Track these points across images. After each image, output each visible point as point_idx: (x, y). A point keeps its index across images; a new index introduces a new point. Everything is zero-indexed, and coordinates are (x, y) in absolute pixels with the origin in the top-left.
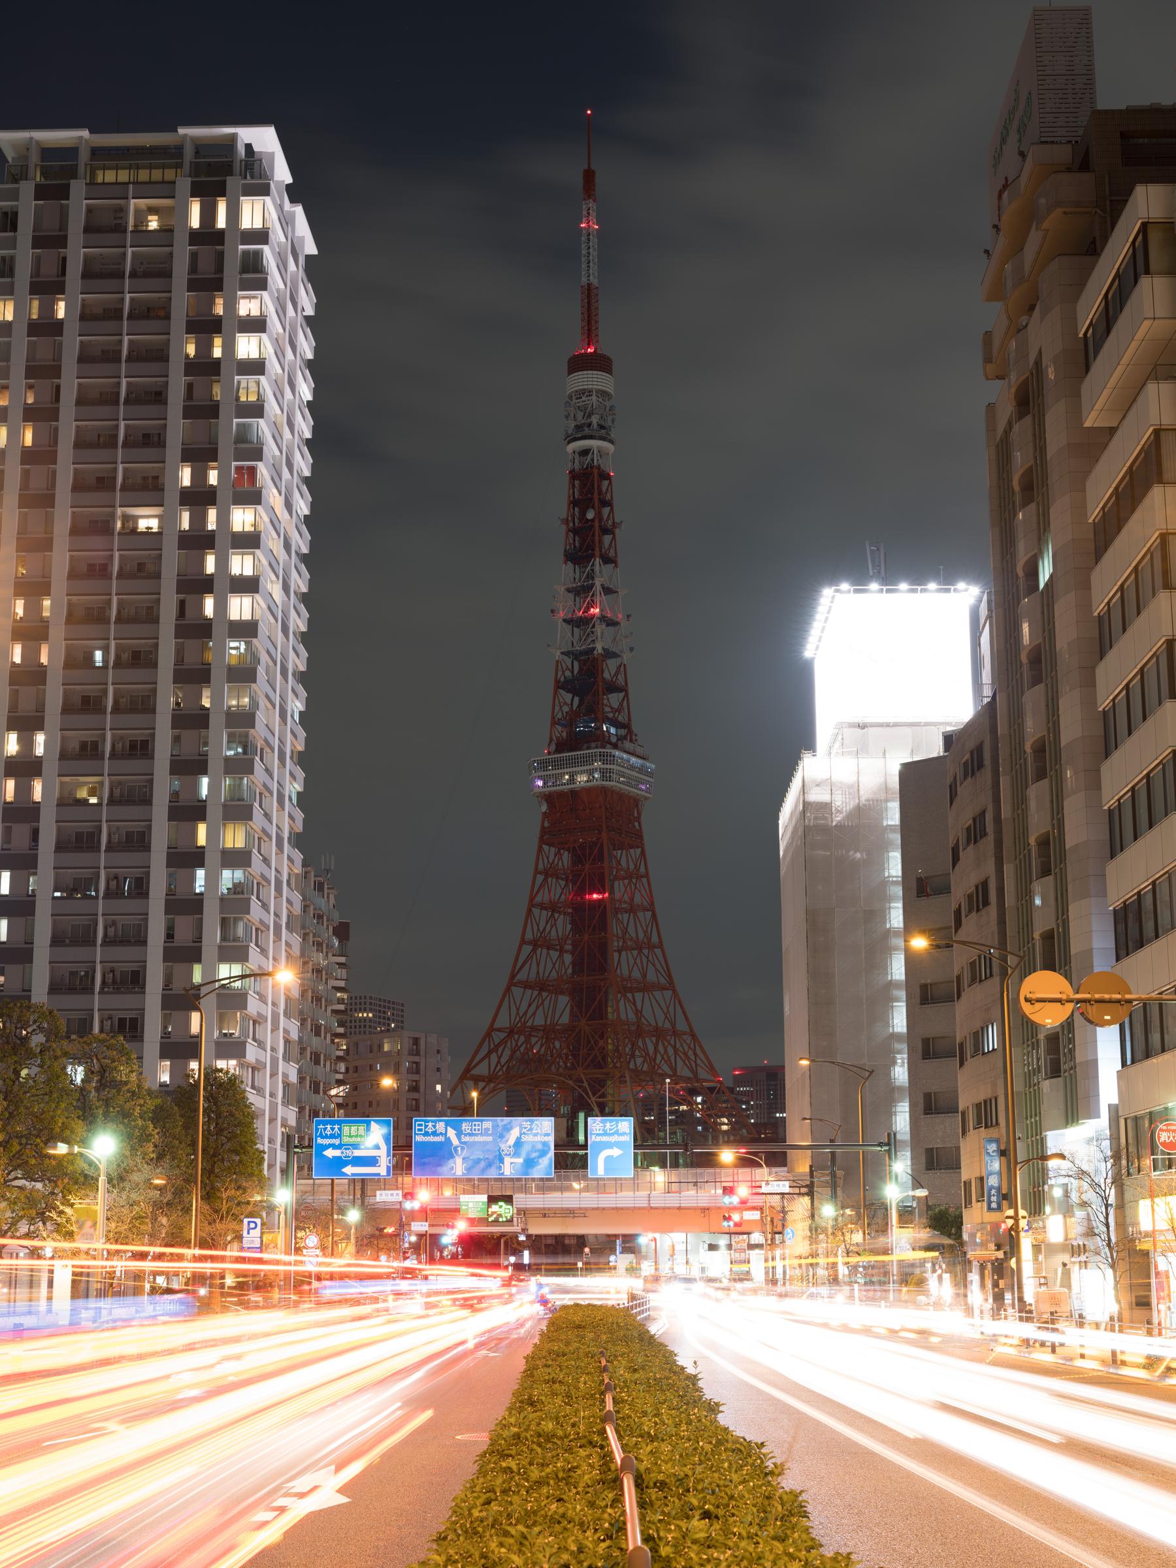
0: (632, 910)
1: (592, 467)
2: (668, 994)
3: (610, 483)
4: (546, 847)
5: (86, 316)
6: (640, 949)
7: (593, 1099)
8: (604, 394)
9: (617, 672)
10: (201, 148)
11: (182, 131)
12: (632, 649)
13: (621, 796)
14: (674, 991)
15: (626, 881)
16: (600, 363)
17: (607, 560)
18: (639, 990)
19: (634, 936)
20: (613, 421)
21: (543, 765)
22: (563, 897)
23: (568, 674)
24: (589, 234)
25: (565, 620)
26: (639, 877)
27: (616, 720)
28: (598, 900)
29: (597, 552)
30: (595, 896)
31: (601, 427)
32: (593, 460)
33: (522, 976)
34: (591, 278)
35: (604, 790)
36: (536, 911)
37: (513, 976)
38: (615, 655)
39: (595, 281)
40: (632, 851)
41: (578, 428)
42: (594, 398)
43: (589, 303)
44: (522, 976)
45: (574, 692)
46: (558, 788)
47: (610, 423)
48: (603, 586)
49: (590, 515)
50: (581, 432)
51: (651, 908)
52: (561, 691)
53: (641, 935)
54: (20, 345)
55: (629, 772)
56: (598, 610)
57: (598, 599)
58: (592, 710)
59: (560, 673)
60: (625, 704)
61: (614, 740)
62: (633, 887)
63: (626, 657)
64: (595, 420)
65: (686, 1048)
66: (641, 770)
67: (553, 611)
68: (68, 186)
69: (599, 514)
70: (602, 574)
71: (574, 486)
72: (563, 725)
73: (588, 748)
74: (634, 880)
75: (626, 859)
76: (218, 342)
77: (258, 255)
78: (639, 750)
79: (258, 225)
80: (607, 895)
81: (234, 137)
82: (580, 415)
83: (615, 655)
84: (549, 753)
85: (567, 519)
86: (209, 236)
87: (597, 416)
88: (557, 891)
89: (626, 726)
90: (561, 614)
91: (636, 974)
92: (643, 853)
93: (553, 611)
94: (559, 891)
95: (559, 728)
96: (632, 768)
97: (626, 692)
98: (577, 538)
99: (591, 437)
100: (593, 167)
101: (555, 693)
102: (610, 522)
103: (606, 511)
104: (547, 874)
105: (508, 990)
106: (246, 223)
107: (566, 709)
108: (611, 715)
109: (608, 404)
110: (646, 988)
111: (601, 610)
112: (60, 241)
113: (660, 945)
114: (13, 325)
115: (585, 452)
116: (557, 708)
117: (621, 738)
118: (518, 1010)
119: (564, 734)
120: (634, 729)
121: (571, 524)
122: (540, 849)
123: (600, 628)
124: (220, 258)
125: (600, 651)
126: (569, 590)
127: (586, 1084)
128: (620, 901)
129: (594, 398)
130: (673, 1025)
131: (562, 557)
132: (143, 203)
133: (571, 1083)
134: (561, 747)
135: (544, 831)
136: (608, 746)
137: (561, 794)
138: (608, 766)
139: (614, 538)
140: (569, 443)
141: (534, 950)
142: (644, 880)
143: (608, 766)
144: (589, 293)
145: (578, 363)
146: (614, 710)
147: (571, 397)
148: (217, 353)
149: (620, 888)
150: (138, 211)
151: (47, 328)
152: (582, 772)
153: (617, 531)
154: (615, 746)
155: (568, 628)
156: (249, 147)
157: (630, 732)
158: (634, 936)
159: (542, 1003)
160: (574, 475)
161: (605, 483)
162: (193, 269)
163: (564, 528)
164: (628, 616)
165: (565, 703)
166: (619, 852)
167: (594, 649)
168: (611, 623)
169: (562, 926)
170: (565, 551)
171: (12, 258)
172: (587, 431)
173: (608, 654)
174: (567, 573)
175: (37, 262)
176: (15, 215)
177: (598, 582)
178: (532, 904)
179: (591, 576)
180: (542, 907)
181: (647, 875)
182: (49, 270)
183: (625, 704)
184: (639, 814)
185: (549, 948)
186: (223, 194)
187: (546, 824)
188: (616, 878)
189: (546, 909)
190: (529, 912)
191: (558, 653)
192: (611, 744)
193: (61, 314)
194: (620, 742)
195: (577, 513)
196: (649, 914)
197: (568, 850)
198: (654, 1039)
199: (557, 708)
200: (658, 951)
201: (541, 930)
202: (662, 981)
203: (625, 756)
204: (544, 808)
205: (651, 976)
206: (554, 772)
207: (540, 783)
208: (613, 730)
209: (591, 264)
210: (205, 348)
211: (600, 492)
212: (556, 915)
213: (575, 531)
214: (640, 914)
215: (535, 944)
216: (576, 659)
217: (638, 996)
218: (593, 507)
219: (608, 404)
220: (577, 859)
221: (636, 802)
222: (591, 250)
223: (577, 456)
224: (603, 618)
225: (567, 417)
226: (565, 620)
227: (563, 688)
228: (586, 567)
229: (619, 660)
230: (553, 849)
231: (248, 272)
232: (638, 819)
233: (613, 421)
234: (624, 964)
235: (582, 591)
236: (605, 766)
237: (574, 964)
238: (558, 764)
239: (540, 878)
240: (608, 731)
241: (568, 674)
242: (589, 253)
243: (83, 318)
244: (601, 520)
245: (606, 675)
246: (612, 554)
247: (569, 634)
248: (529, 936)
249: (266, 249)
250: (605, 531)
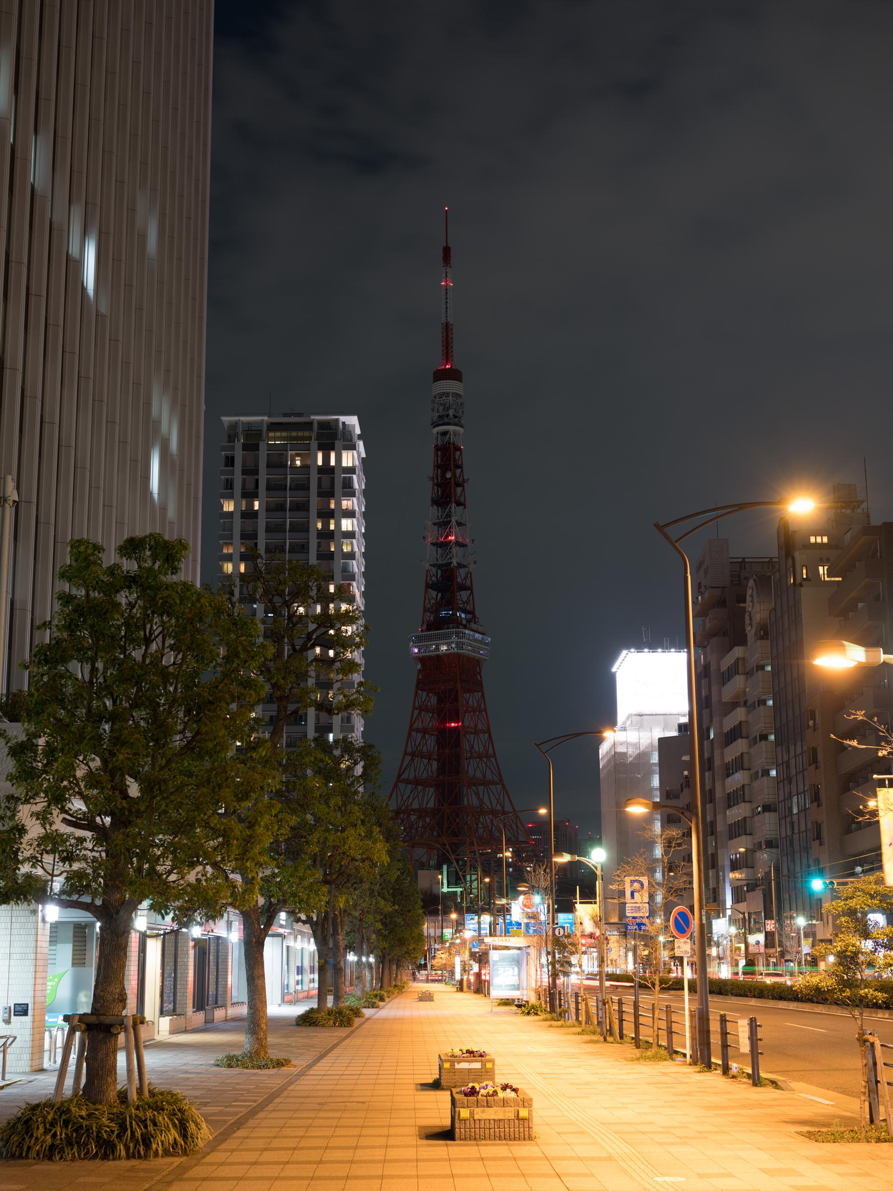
0: (476, 733)
1: (449, 443)
2: (499, 787)
3: (461, 454)
4: (420, 692)
5: (269, 508)
6: (481, 758)
7: (453, 857)
8: (457, 395)
9: (466, 578)
10: (324, 425)
11: (312, 417)
12: (475, 562)
13: (469, 659)
14: (503, 785)
15: (472, 714)
16: (454, 375)
17: (459, 504)
18: (481, 785)
19: (477, 750)
20: (463, 413)
21: (419, 639)
22: (431, 723)
23: (434, 579)
24: (447, 290)
25: (432, 544)
26: (480, 711)
27: (466, 609)
28: (455, 727)
29: (453, 500)
30: (453, 725)
31: (455, 417)
32: (450, 438)
33: (405, 776)
34: (448, 318)
35: (458, 655)
36: (414, 734)
37: (399, 776)
38: (464, 566)
39: (451, 320)
40: (476, 694)
41: (439, 417)
42: (451, 398)
43: (447, 335)
44: (405, 776)
45: (438, 590)
46: (427, 654)
47: (461, 414)
48: (457, 522)
49: (448, 475)
50: (442, 420)
51: (488, 731)
52: (430, 590)
53: (481, 749)
54: (237, 522)
55: (474, 643)
56: (453, 538)
57: (453, 530)
58: (449, 602)
59: (429, 578)
60: (471, 598)
61: (464, 622)
62: (476, 717)
63: (472, 567)
64: (451, 412)
65: (511, 822)
66: (481, 642)
67: (424, 538)
68: (258, 444)
69: (454, 475)
70: (457, 513)
71: (437, 455)
72: (432, 613)
73: (448, 628)
74: (477, 713)
75: (472, 699)
76: (332, 522)
77: (351, 479)
78: (480, 629)
79: (350, 465)
80: (460, 724)
81: (337, 420)
82: (441, 408)
83: (464, 566)
84: (422, 631)
85: (433, 478)
86: (326, 469)
88: (428, 720)
89: (472, 613)
90: (430, 540)
91: (479, 774)
92: (483, 695)
93: (424, 538)
94: (428, 719)
95: (428, 614)
96: (476, 640)
97: (472, 590)
98: (440, 489)
99: (449, 424)
100: (449, 245)
101: (426, 591)
102: (461, 480)
103: (458, 471)
104: (420, 709)
105: (396, 785)
106: (344, 464)
107: (433, 601)
108: (462, 606)
109: (459, 401)
110: (485, 783)
111: (456, 537)
112: (256, 472)
113: (494, 756)
114: (234, 514)
115: (445, 433)
116: (427, 601)
117: (469, 621)
118: (402, 796)
119: (432, 618)
120: (477, 613)
121: (436, 481)
122: (416, 693)
123: (455, 550)
124: (333, 479)
125: (455, 564)
126: (434, 524)
127: (448, 847)
128: (469, 727)
129: (451, 398)
130: (503, 807)
131: (429, 502)
132: (294, 452)
133: (438, 846)
134: (430, 626)
135: (419, 682)
136: (461, 626)
137: (430, 658)
138: (461, 640)
139: (463, 490)
140: (434, 427)
141: (412, 760)
142: (484, 713)
143: (461, 640)
144: (447, 328)
145: (440, 375)
146: (464, 603)
147: (435, 397)
148: (332, 527)
149: (468, 717)
150: (291, 455)
151: (249, 514)
152: (444, 644)
153: (465, 485)
154: (465, 627)
155: (433, 547)
156: (344, 423)
157: (474, 616)
158: (477, 750)
159: (418, 795)
160: (437, 448)
161: (458, 453)
162: (319, 486)
163: (431, 483)
164: (473, 541)
165: (432, 598)
166: (468, 694)
167: (451, 563)
168: (462, 545)
169: (431, 744)
170: (432, 498)
171: (232, 480)
172: (446, 420)
173: (460, 566)
174: (433, 512)
175: (244, 481)
176: (233, 458)
177: (453, 519)
178: (411, 729)
179: (449, 515)
180: (418, 731)
181: (485, 710)
182: (250, 486)
183: (471, 598)
184: (480, 670)
185: (422, 757)
186: (333, 449)
187: (420, 677)
188: (466, 712)
189: (420, 732)
190: (409, 734)
191: (428, 565)
192: (462, 625)
193: (256, 508)
194: (468, 624)
195: (439, 473)
196: (487, 735)
197: (435, 693)
198: (491, 816)
199: (427, 601)
200: (493, 759)
201: (417, 744)
202: (496, 779)
203: (471, 633)
204: (419, 666)
205: (489, 776)
206: (426, 643)
207: (416, 650)
208: (463, 616)
209: (448, 309)
210: (326, 525)
211: (455, 459)
212: (427, 736)
213: (438, 485)
214: (481, 735)
215: (413, 755)
216: (439, 568)
217: (481, 788)
218: (450, 470)
219: (459, 401)
220: (440, 700)
221: (478, 662)
222: (448, 300)
223: (439, 436)
224: (458, 544)
225: (433, 410)
226: (432, 544)
227: (429, 588)
228: (446, 509)
229: (467, 570)
230: (425, 693)
231: (346, 488)
232: (480, 673)
233: (463, 413)
234: (472, 769)
235: (444, 524)
236: (459, 640)
237: (438, 769)
238: (429, 638)
239: (416, 712)
240: (460, 616)
241: (434, 579)
242: (447, 302)
243: (267, 510)
244: (455, 477)
245: (459, 580)
246: (462, 500)
247: (435, 553)
248: (409, 750)
249: (355, 477)
250: (458, 485)
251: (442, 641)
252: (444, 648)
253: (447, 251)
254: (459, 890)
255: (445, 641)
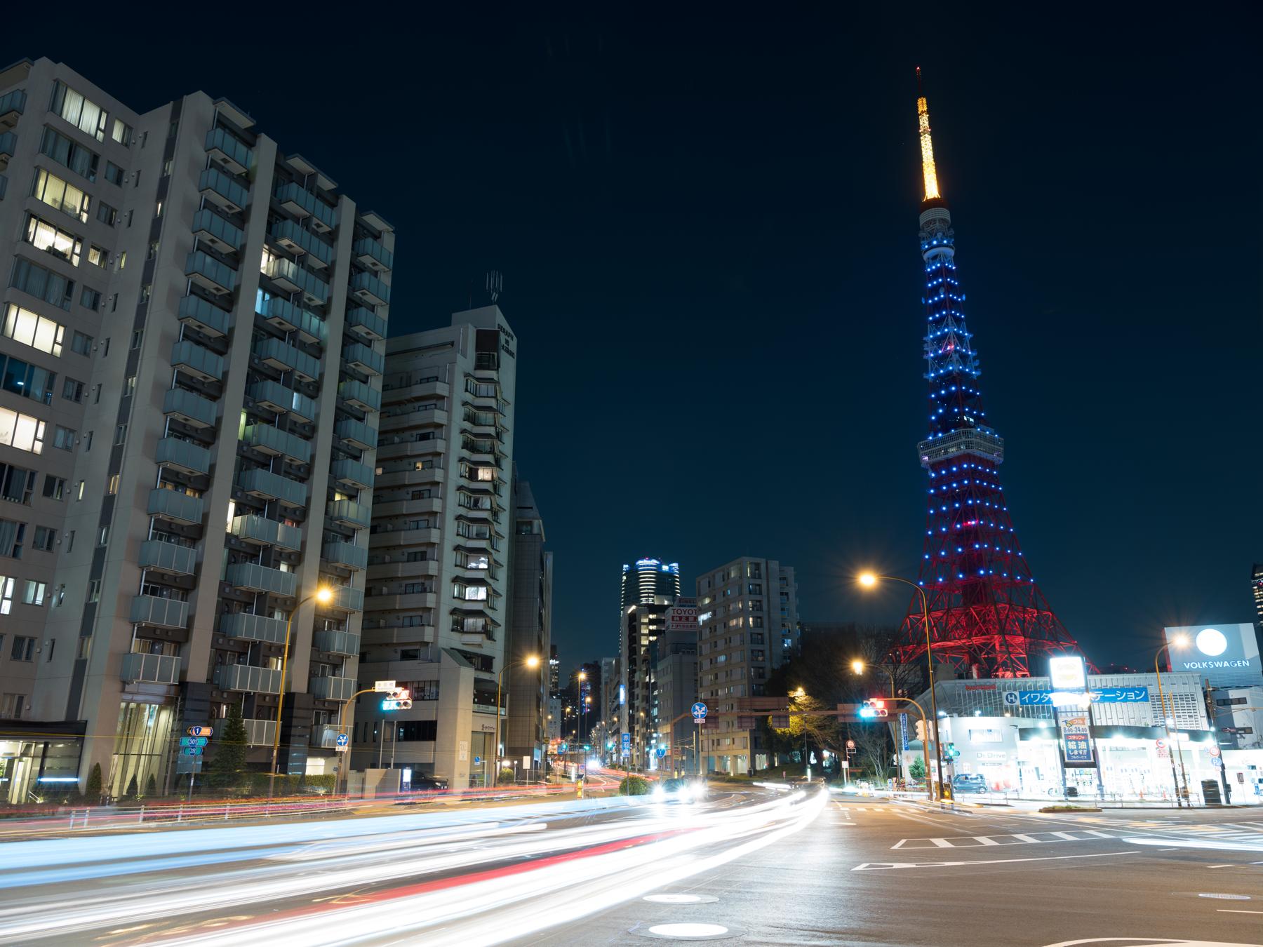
42: (937, 224)
87: (941, 234)
129: (937, 224)
138: (969, 439)
143: (969, 439)
207: (926, 458)
223: (930, 261)
236: (967, 440)
240: (968, 420)
251: (950, 444)
255: (953, 443)
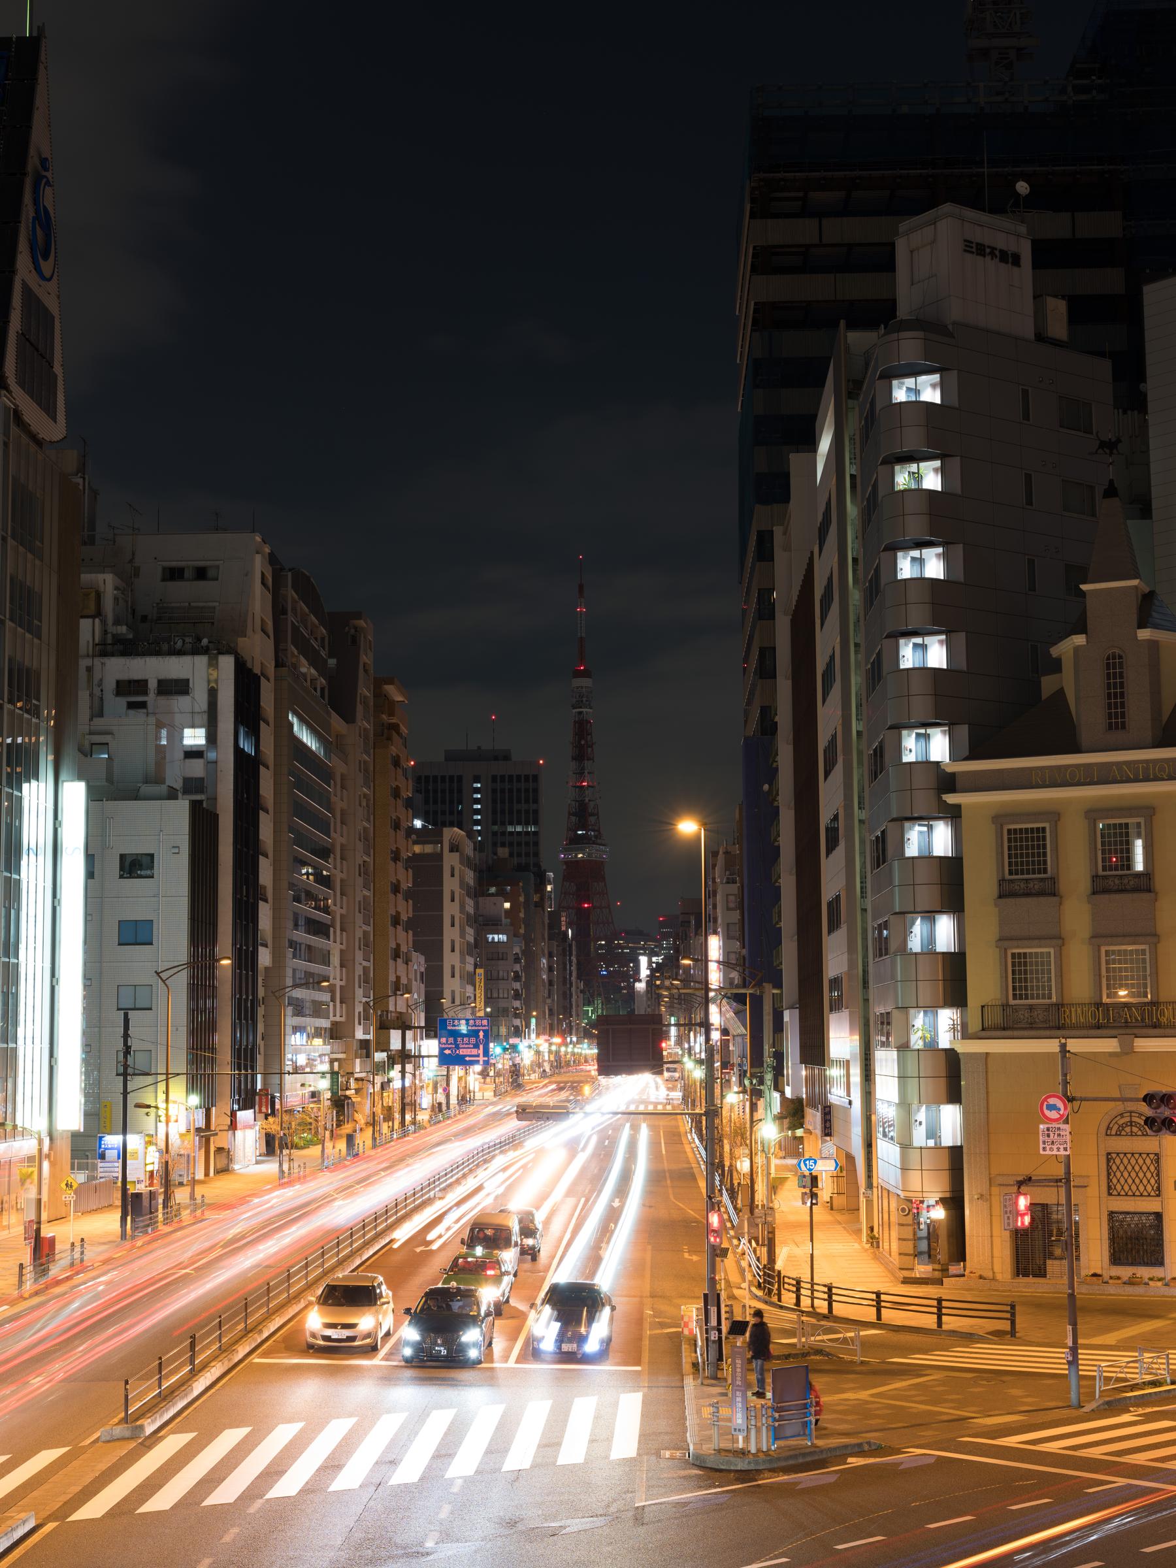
16: (586, 674)
21: (566, 850)
49: (583, 742)
89: (599, 831)
92: (605, 885)
115: (580, 713)
117: (596, 837)
137: (571, 862)
145: (578, 674)
154: (594, 843)
179: (583, 769)
224: (588, 786)
235: (580, 774)
252: (580, 856)
253: (581, 587)
254: (590, 1009)
